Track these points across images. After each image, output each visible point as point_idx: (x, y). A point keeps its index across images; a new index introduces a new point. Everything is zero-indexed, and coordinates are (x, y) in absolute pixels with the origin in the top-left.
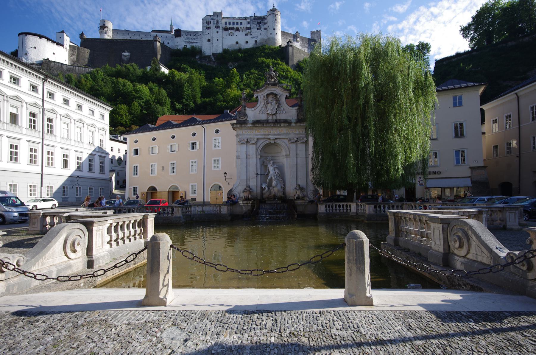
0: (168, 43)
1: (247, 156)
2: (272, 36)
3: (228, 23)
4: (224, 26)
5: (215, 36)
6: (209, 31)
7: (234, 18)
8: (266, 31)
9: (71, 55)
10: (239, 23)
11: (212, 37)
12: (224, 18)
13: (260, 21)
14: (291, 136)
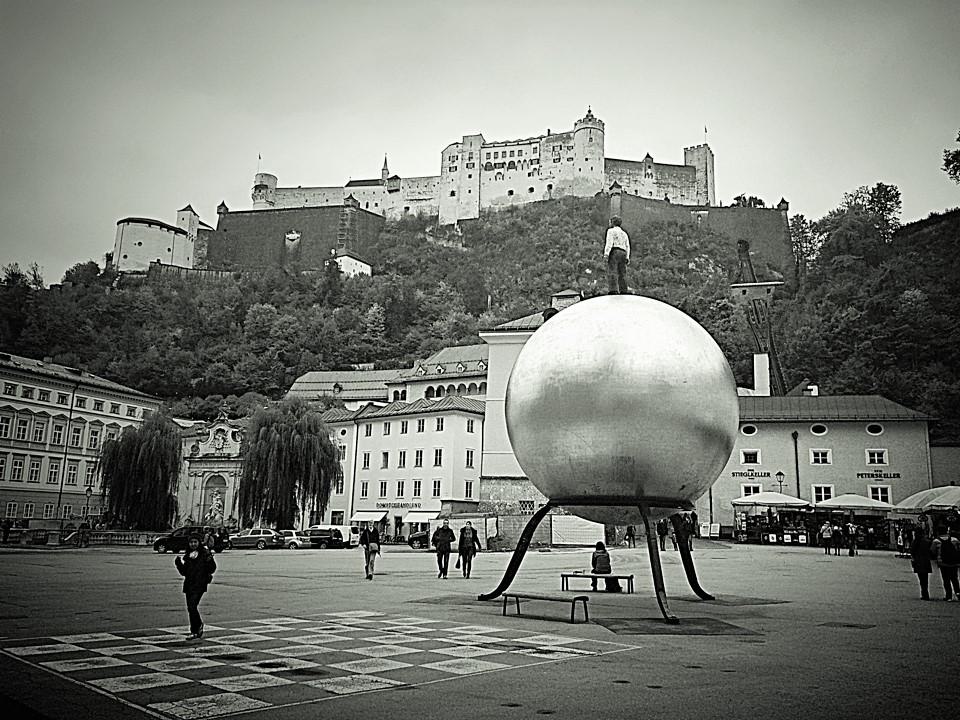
0: (376, 205)
1: (195, 488)
3: (492, 155)
5: (466, 183)
7: (506, 144)
9: (198, 248)
10: (516, 153)
14: (231, 470)
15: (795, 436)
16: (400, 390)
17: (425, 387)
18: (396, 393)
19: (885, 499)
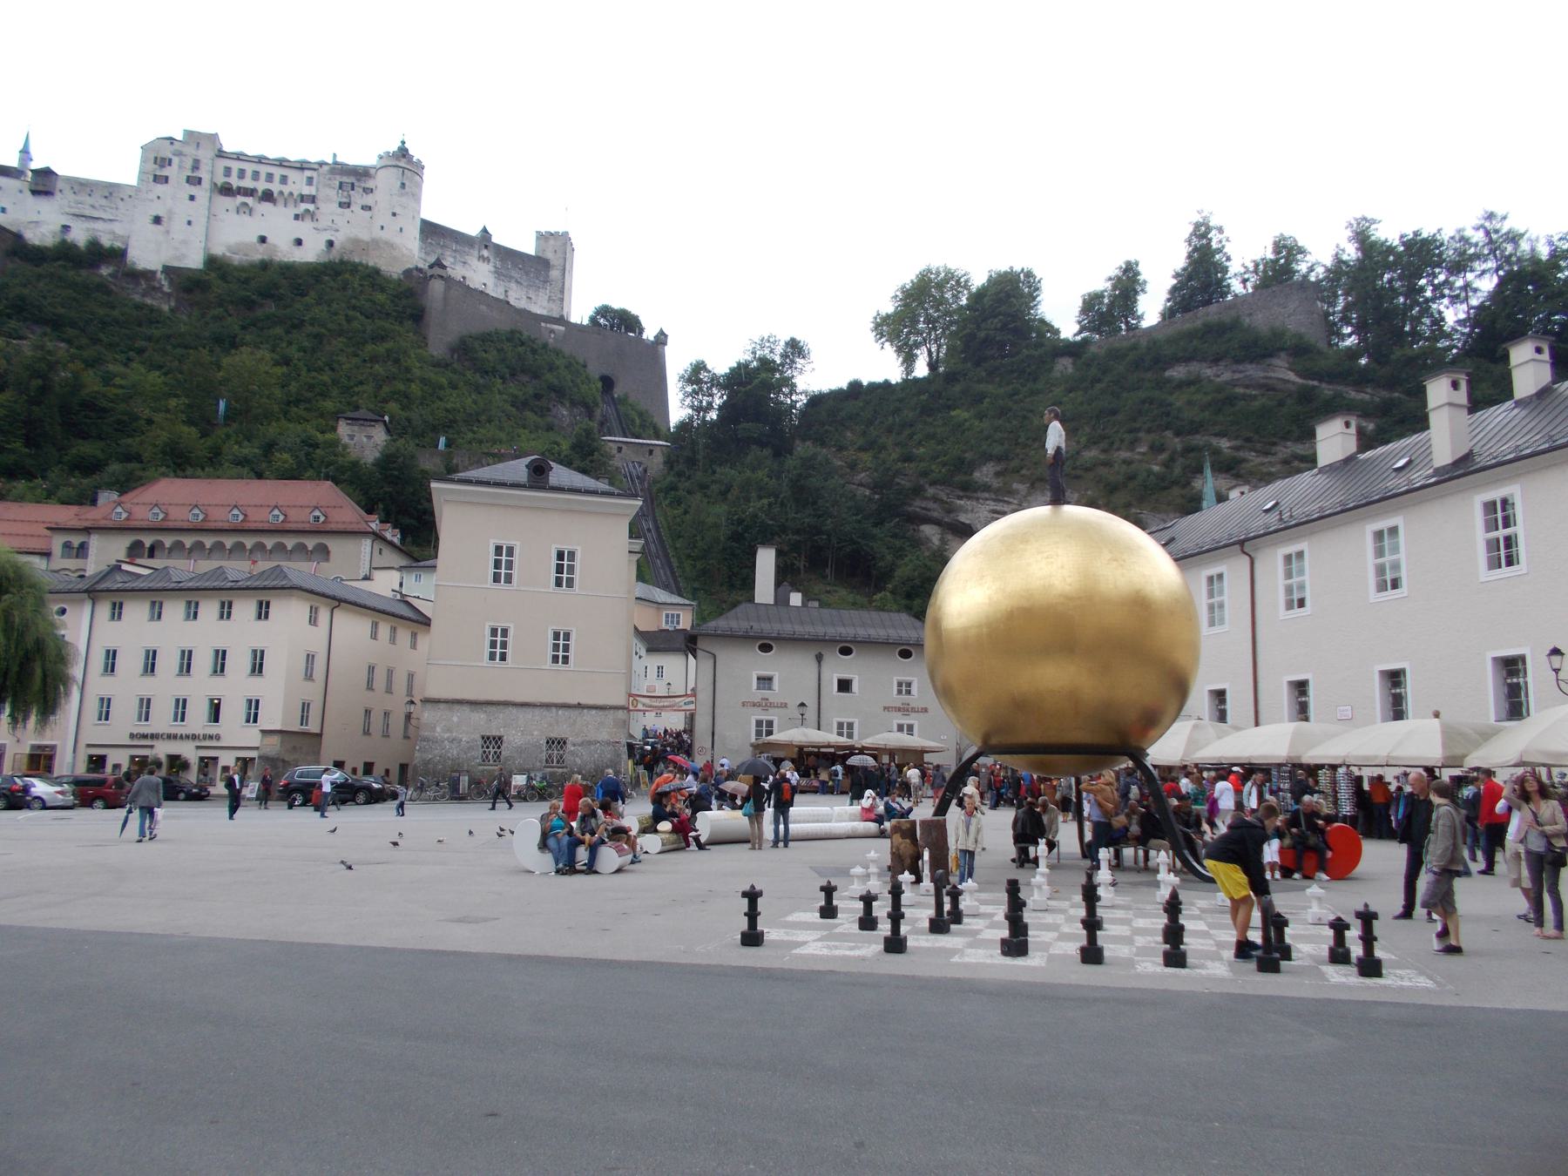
2: (384, 235)
3: (235, 173)
4: (220, 180)
5: (184, 209)
6: (160, 189)
7: (261, 160)
8: (367, 214)
10: (277, 178)
11: (170, 212)
12: (221, 154)
13: (352, 178)
15: (819, 658)
16: (76, 540)
17: (125, 541)
18: (67, 545)
19: (850, 736)
